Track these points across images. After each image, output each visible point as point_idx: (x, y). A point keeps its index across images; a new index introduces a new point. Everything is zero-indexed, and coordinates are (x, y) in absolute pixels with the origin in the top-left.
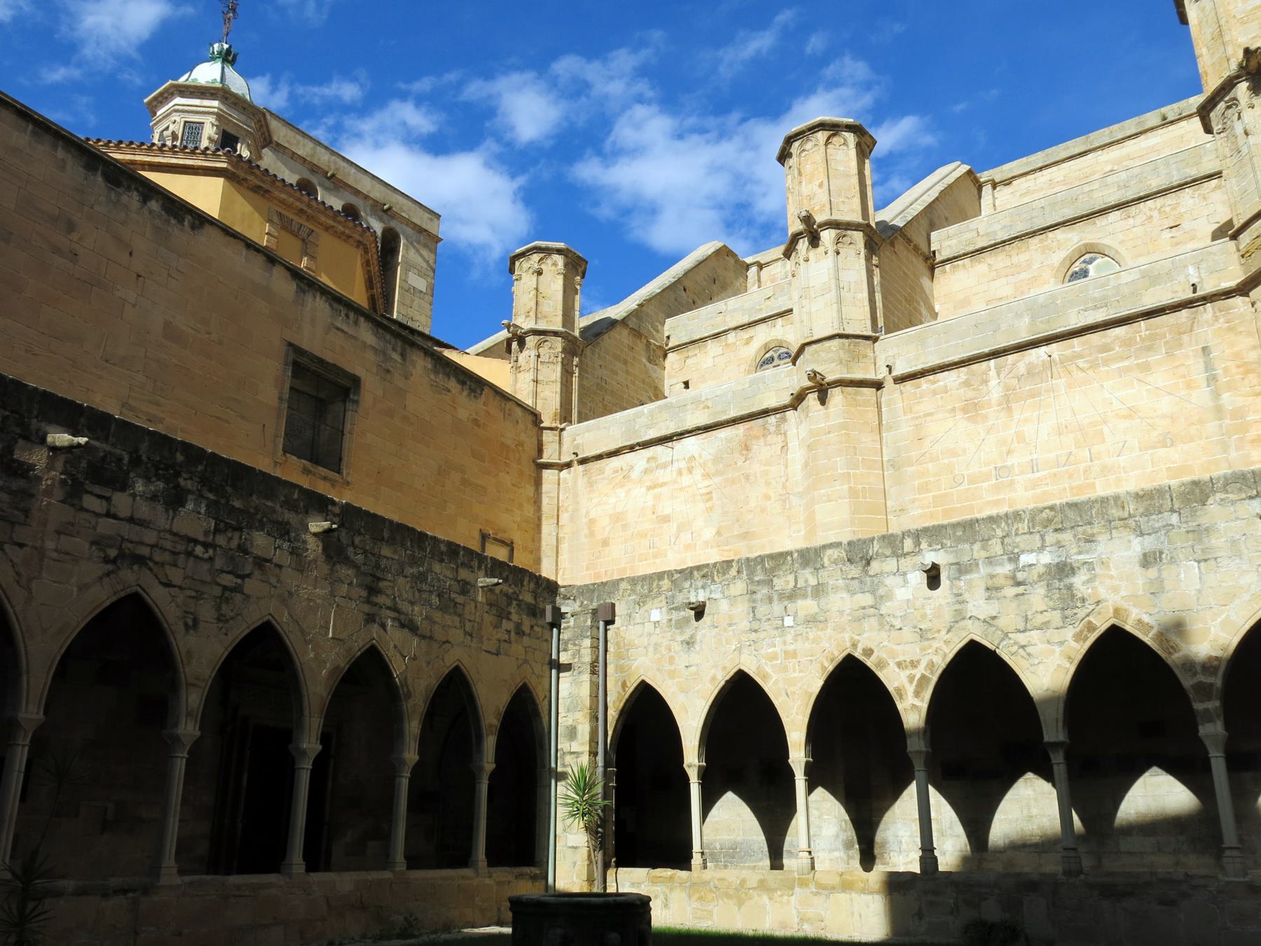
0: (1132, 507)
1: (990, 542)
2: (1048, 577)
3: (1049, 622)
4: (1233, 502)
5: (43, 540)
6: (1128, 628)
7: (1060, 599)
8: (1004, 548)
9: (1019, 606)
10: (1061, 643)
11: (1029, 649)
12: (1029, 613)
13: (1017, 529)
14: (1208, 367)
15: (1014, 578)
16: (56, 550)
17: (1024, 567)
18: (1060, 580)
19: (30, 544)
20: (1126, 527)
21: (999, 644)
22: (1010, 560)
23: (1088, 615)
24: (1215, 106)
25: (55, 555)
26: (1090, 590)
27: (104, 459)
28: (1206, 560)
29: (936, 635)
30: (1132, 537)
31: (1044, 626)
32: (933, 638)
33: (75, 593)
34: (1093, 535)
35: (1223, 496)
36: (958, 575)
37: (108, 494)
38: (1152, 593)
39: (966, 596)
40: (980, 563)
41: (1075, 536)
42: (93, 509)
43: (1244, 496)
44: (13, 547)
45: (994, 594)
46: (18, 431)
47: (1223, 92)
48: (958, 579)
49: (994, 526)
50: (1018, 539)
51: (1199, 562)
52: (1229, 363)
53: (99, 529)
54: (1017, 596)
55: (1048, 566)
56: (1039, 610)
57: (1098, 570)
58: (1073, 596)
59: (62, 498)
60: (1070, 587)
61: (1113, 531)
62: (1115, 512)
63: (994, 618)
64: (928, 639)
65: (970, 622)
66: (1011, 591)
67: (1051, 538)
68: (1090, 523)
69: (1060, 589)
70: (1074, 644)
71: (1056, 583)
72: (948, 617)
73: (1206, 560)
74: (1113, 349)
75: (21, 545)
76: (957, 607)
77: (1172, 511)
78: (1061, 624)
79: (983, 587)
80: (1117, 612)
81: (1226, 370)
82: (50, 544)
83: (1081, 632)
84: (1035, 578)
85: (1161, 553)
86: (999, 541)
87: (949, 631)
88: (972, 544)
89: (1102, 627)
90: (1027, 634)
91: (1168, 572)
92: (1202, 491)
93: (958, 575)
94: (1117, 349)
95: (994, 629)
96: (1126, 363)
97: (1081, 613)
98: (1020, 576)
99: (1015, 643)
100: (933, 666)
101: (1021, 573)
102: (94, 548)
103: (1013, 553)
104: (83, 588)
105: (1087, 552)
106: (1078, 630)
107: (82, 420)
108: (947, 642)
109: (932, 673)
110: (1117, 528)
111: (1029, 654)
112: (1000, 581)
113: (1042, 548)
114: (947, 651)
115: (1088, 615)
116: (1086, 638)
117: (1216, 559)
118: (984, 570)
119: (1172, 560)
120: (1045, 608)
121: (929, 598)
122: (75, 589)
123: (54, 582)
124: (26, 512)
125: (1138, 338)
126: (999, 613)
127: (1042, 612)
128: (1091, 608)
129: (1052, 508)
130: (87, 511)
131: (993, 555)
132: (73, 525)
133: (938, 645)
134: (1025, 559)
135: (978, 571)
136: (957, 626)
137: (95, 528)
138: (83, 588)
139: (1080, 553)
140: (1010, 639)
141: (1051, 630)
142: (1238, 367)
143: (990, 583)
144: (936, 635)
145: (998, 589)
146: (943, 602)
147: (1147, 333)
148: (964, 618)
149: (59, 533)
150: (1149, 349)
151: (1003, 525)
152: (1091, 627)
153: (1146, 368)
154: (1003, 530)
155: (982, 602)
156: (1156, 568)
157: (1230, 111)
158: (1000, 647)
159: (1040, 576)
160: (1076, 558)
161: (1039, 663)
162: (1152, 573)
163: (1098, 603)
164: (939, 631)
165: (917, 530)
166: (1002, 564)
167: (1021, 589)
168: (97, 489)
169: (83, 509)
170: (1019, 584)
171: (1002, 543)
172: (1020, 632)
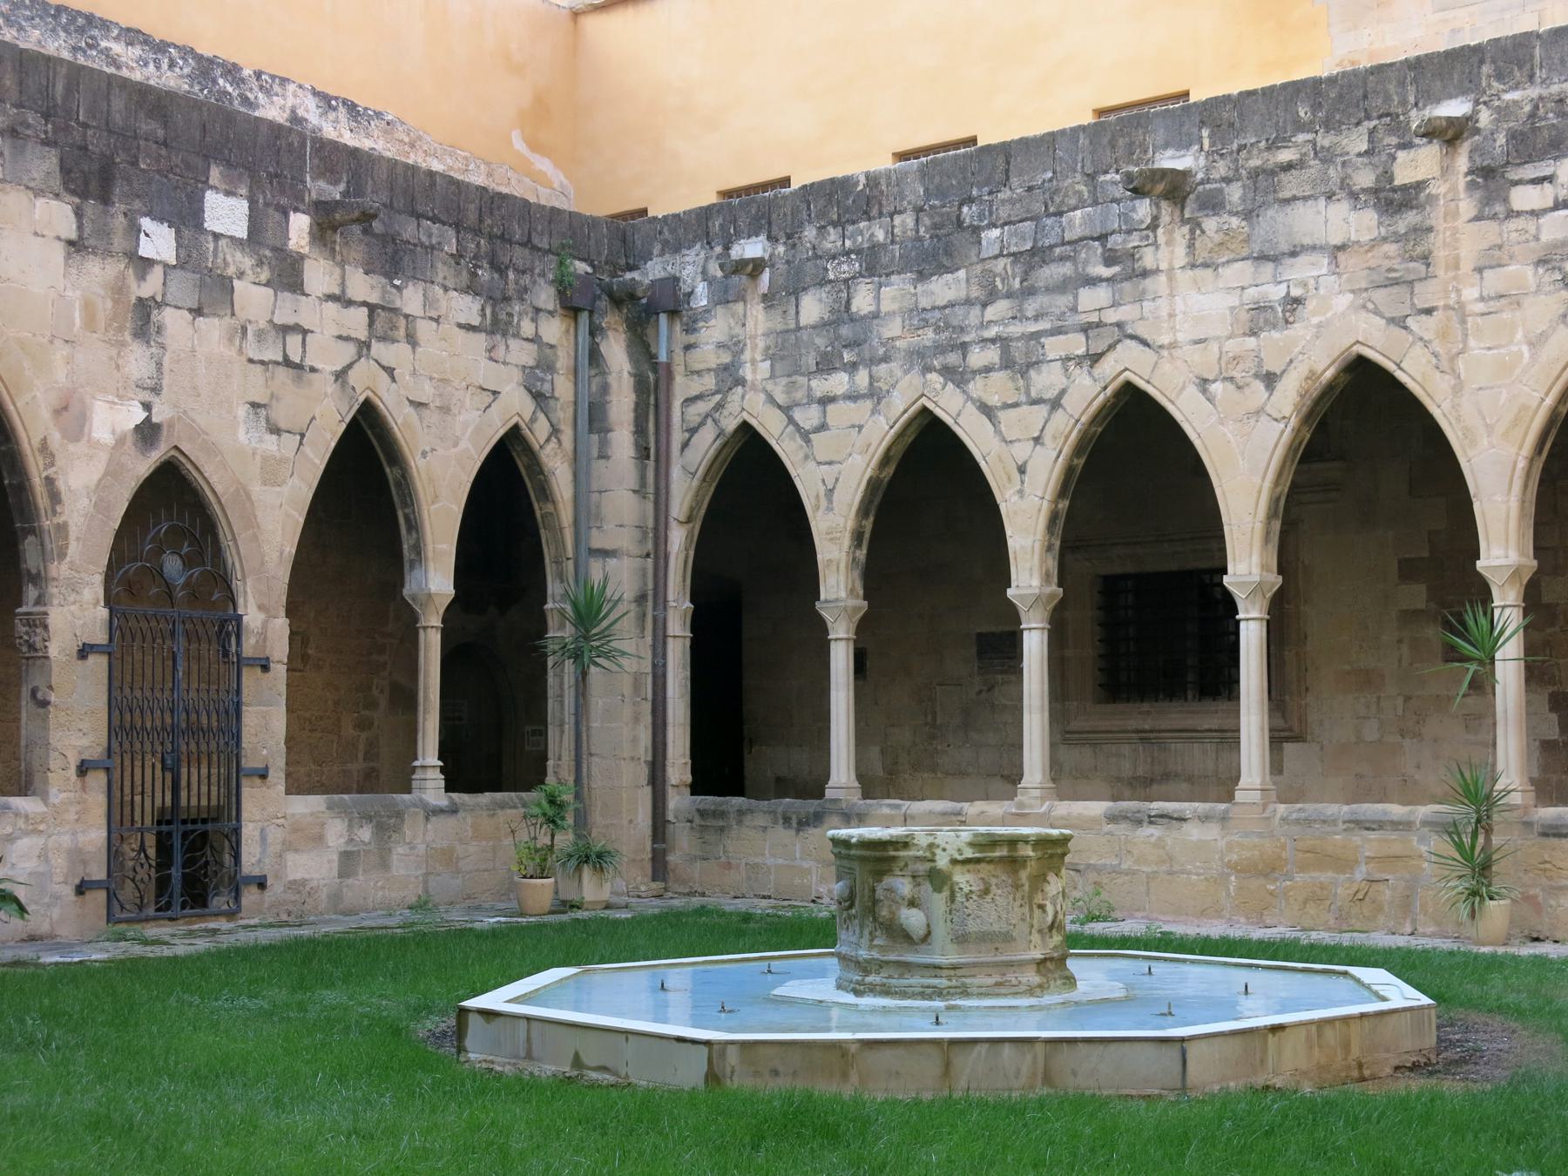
5: (1458, 291)
16: (1482, 299)
19: (1441, 303)
25: (1480, 307)
27: (1536, 107)
33: (1526, 355)
37: (1547, 172)
42: (1528, 208)
44: (1419, 318)
46: (1394, 140)
53: (1544, 238)
59: (1473, 213)
75: (1429, 311)
82: (1470, 293)
102: (1541, 271)
104: (1536, 342)
107: (1486, 69)
122: (1525, 349)
123: (1489, 349)
124: (1426, 258)
130: (1519, 214)
132: (1500, 247)
137: (1537, 238)
138: (1536, 342)
149: (1480, 270)
168: (1530, 172)
169: (1512, 214)
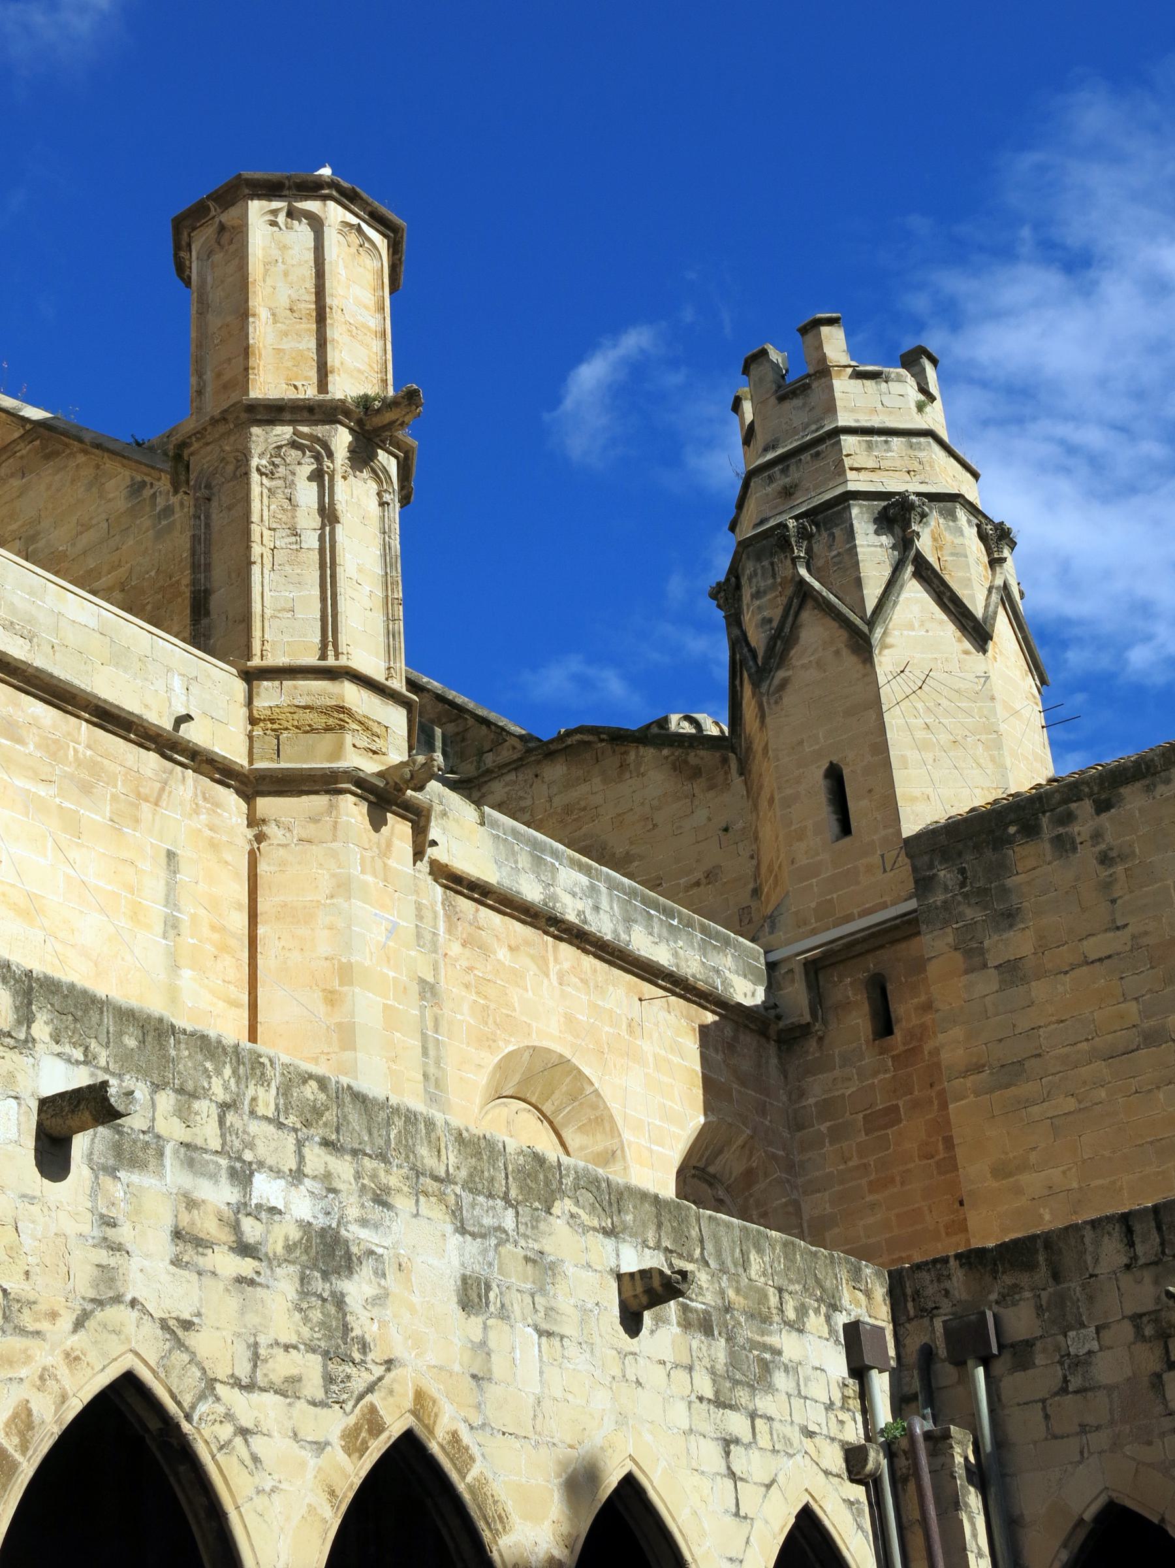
0: (452, 1157)
1: (196, 1105)
2: (304, 1258)
3: (300, 1380)
4: (586, 1229)
6: (434, 1448)
7: (322, 1324)
8: (223, 1136)
9: (243, 1311)
10: (320, 1447)
11: (257, 1442)
12: (263, 1340)
13: (254, 1099)
14: (171, 899)
15: (236, 1227)
17: (259, 1206)
18: (325, 1276)
20: (441, 1197)
21: (193, 1407)
22: (233, 1174)
23: (370, 1389)
24: (272, 422)
26: (375, 1327)
28: (549, 1334)
29: (44, 1326)
30: (449, 1228)
31: (288, 1389)
32: (38, 1333)
34: (387, 1190)
35: (575, 1210)
36: (111, 1162)
38: (474, 1376)
39: (124, 1234)
40: (169, 1150)
41: (358, 1176)
43: (596, 1223)
45: (189, 1255)
47: (306, 414)
48: (112, 1172)
49: (208, 1065)
50: (255, 1127)
51: (541, 1333)
52: (202, 912)
54: (240, 1280)
55: (305, 1226)
56: (284, 1339)
57: (390, 1281)
58: (346, 1329)
60: (339, 1301)
61: (422, 1199)
62: (427, 1159)
63: (187, 1325)
64: (21, 1331)
65: (135, 1314)
66: (230, 1265)
67: (316, 1158)
68: (383, 1157)
69: (324, 1300)
70: (342, 1457)
71: (319, 1285)
72: (83, 1284)
73: (549, 1334)
74: (20, 741)
76: (103, 1256)
77: (506, 1198)
78: (320, 1395)
79: (168, 1223)
80: (420, 1396)
81: (194, 918)
83: (357, 1429)
84: (280, 1250)
85: (488, 1288)
86: (214, 1111)
87: (79, 1324)
88: (156, 1087)
89: (395, 1429)
90: (256, 1397)
91: (499, 1336)
92: (547, 1183)
93: (111, 1162)
94: (31, 747)
95: (186, 1357)
96: (42, 791)
97: (360, 1380)
98: (252, 1230)
99: (229, 1416)
100: (30, 1426)
101: (250, 1219)
103: (239, 1159)
105: (376, 1227)
106: (352, 1420)
108: (72, 1359)
109: (24, 1447)
110: (426, 1194)
111: (256, 1459)
112: (209, 1227)
113: (297, 1176)
114: (68, 1383)
115: (370, 1389)
116: (362, 1450)
117: (562, 1337)
118: (174, 1175)
119: (504, 1314)
120: (294, 1340)
121: (31, 1199)
125: (71, 752)
126: (199, 1315)
127: (287, 1348)
128: (378, 1371)
129: (322, 1083)
131: (199, 1142)
133: (49, 1361)
134: (266, 1188)
135: (160, 1174)
136: (99, 1315)
139: (363, 1222)
140: (218, 1399)
141: (301, 1405)
142: (213, 928)
143: (185, 1220)
144: (44, 1326)
145: (201, 1243)
146: (71, 1228)
147: (89, 753)
148: (117, 1299)
150: (86, 789)
151: (227, 1071)
152: (374, 1424)
153: (73, 826)
154: (226, 1088)
155: (161, 1266)
156: (480, 1319)
157: (295, 454)
158: (196, 1418)
159: (289, 1248)
160: (358, 1235)
161: (273, 1490)
162: (473, 1326)
163: (389, 1364)
164: (53, 1315)
165: (29, 974)
166: (213, 1177)
167: (247, 1266)
170: (245, 1249)
171: (221, 1121)
172: (237, 1383)
